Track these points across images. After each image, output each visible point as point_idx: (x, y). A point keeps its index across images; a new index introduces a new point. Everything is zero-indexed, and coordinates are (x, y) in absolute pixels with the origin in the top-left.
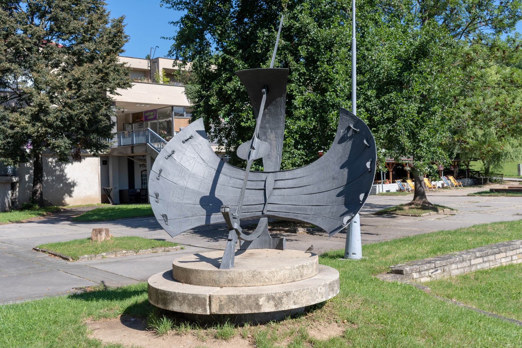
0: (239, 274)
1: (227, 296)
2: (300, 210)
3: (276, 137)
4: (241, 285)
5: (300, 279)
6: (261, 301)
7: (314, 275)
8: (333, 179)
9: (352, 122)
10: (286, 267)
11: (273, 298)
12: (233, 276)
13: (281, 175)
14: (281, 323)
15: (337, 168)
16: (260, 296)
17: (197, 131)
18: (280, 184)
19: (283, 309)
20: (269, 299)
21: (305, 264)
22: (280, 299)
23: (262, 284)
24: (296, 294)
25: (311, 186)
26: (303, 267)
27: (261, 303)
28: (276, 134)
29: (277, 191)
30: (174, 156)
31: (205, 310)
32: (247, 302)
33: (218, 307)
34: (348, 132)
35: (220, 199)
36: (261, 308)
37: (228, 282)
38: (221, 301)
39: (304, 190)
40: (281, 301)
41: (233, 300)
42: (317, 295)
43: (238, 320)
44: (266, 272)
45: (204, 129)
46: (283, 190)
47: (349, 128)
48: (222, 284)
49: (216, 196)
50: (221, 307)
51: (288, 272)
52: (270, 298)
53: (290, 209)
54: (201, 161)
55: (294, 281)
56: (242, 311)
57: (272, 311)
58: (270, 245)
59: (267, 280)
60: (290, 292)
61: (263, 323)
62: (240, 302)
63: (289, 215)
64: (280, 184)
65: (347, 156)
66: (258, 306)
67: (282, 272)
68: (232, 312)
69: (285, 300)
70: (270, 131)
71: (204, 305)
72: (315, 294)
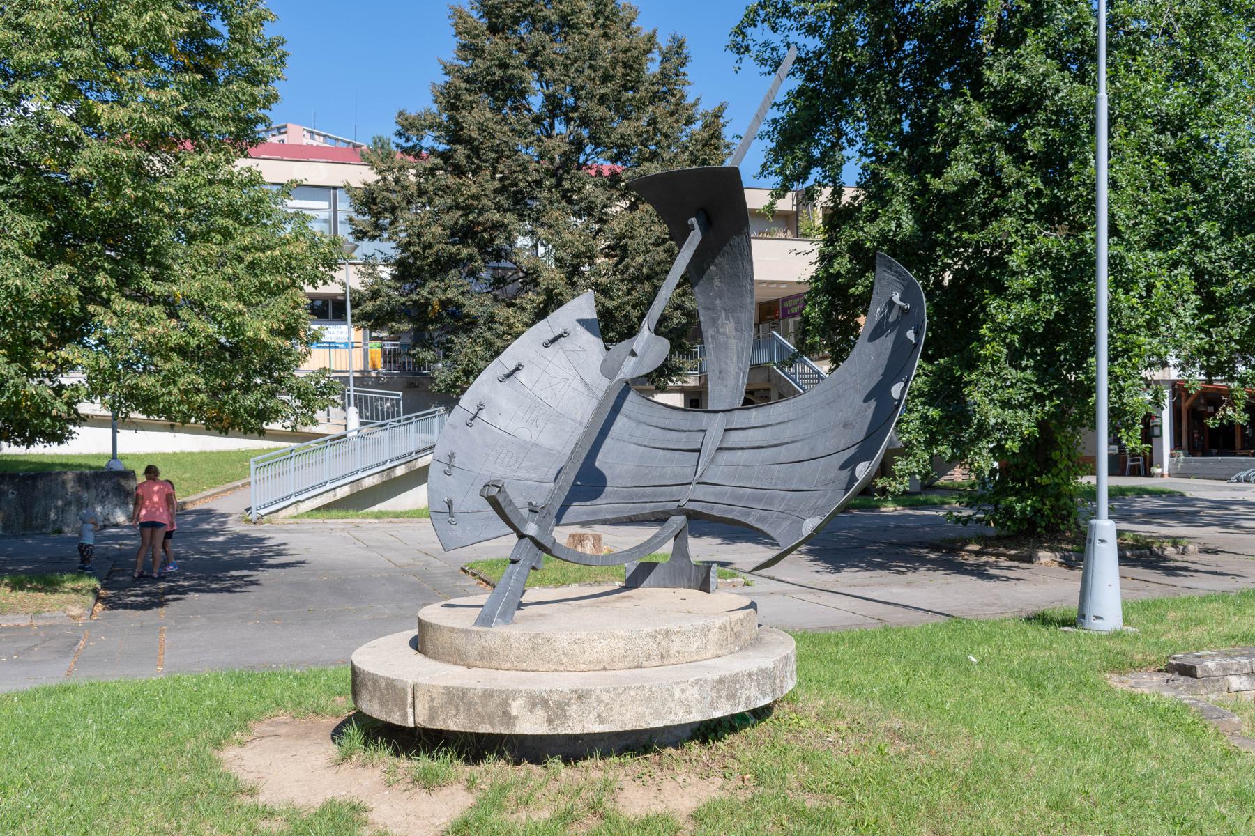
0: (504, 639)
1: (445, 687)
2: (759, 499)
3: (737, 330)
4: (508, 665)
5: (658, 662)
6: (516, 707)
7: (708, 656)
8: (845, 426)
9: (900, 286)
10: (617, 632)
11: (545, 703)
12: (491, 644)
13: (741, 418)
14: (580, 763)
15: (859, 399)
16: (514, 694)
17: (579, 321)
18: (735, 439)
19: (569, 732)
20: (534, 705)
21: (675, 628)
22: (562, 706)
23: (553, 668)
24: (605, 697)
25: (799, 445)
26: (667, 633)
27: (514, 712)
28: (737, 321)
29: (726, 454)
30: (521, 375)
31: (405, 715)
32: (484, 706)
33: (426, 712)
34: (890, 312)
35: (604, 471)
36: (514, 725)
37: (482, 658)
38: (432, 700)
39: (783, 453)
40: (565, 711)
41: (456, 697)
42: (670, 704)
43: (474, 748)
44: (563, 641)
45: (595, 316)
46: (739, 453)
47: (891, 304)
48: (471, 661)
49: (597, 464)
50: (432, 717)
51: (621, 644)
52: (538, 701)
53: (740, 498)
54: (581, 388)
55: (637, 667)
56: (472, 727)
57: (541, 732)
58: (689, 580)
59: (565, 660)
60: (588, 693)
61: (537, 760)
62: (470, 705)
63: (731, 512)
64: (735, 439)
65: (881, 371)
66: (508, 718)
67: (604, 643)
68: (453, 727)
69: (573, 710)
70: (723, 315)
71: (402, 705)
72: (664, 702)
